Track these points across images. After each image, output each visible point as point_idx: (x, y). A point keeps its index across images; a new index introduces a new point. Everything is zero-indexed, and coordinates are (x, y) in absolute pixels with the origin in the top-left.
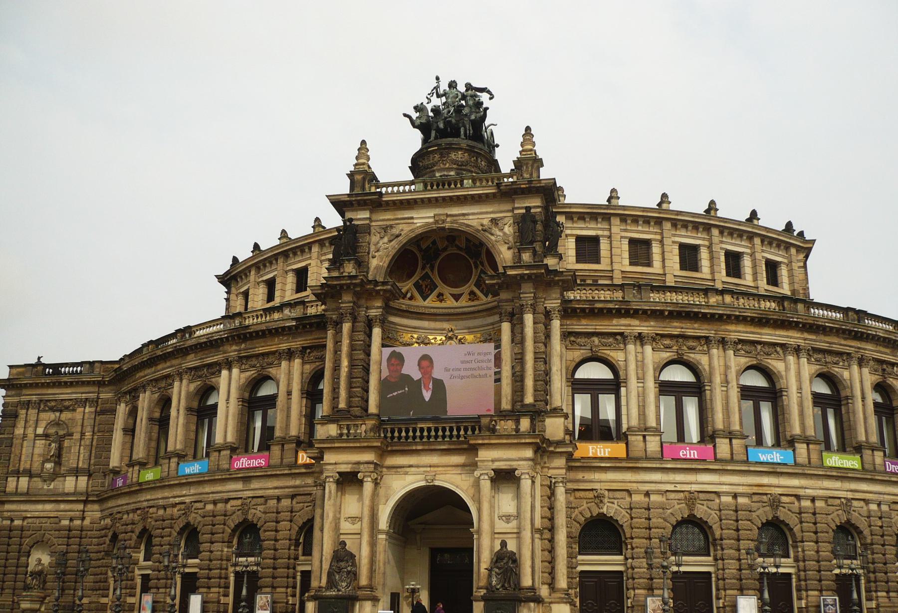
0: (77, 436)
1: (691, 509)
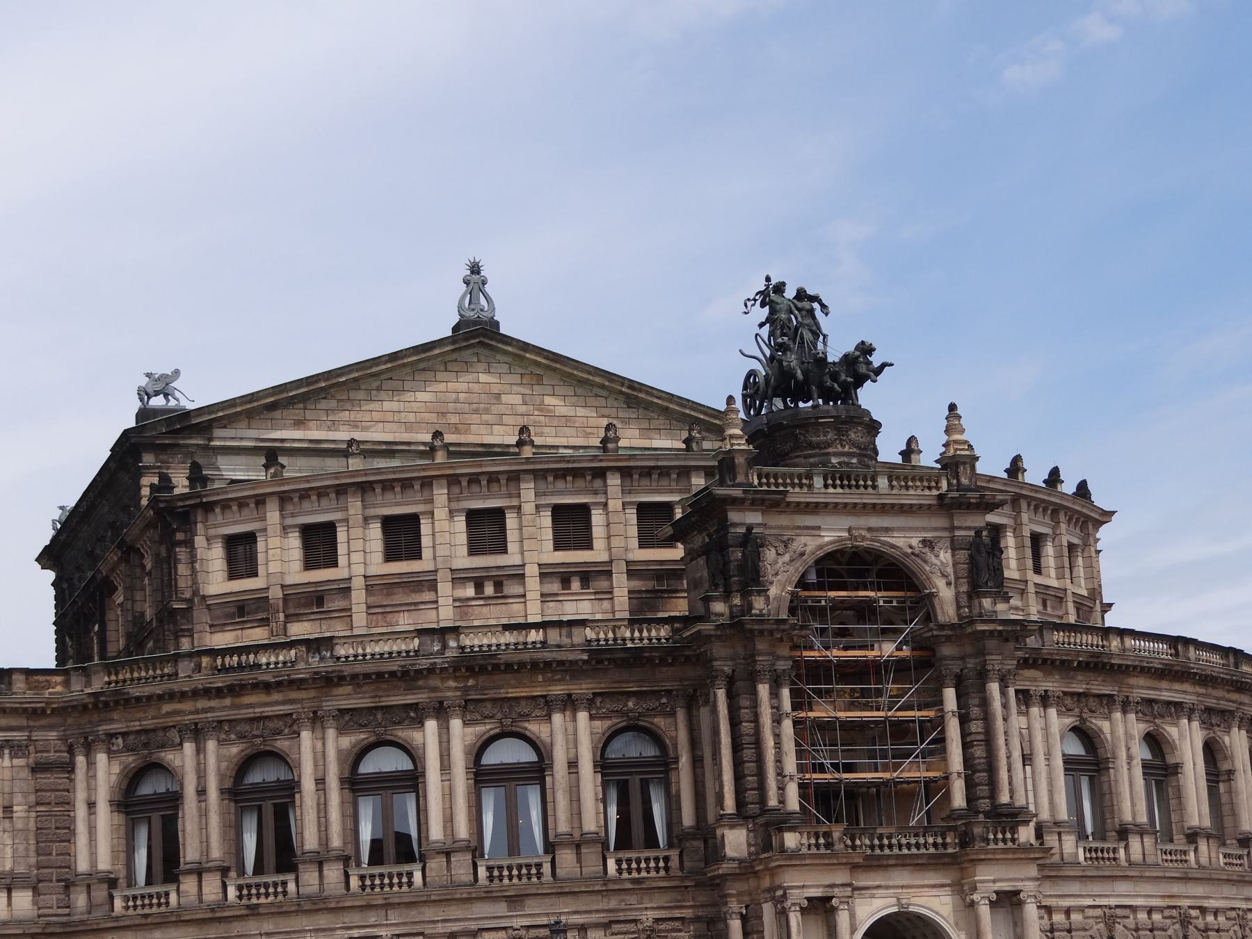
1: (1110, 931)
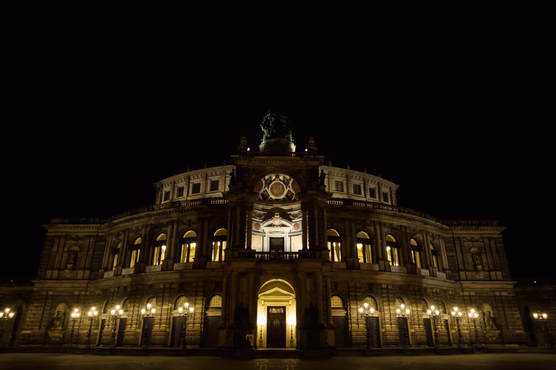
0: (85, 253)
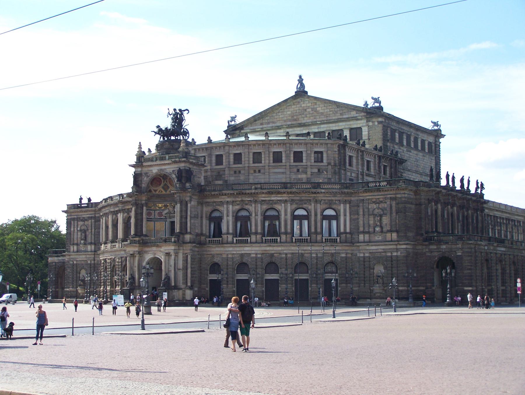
0: (90, 231)
